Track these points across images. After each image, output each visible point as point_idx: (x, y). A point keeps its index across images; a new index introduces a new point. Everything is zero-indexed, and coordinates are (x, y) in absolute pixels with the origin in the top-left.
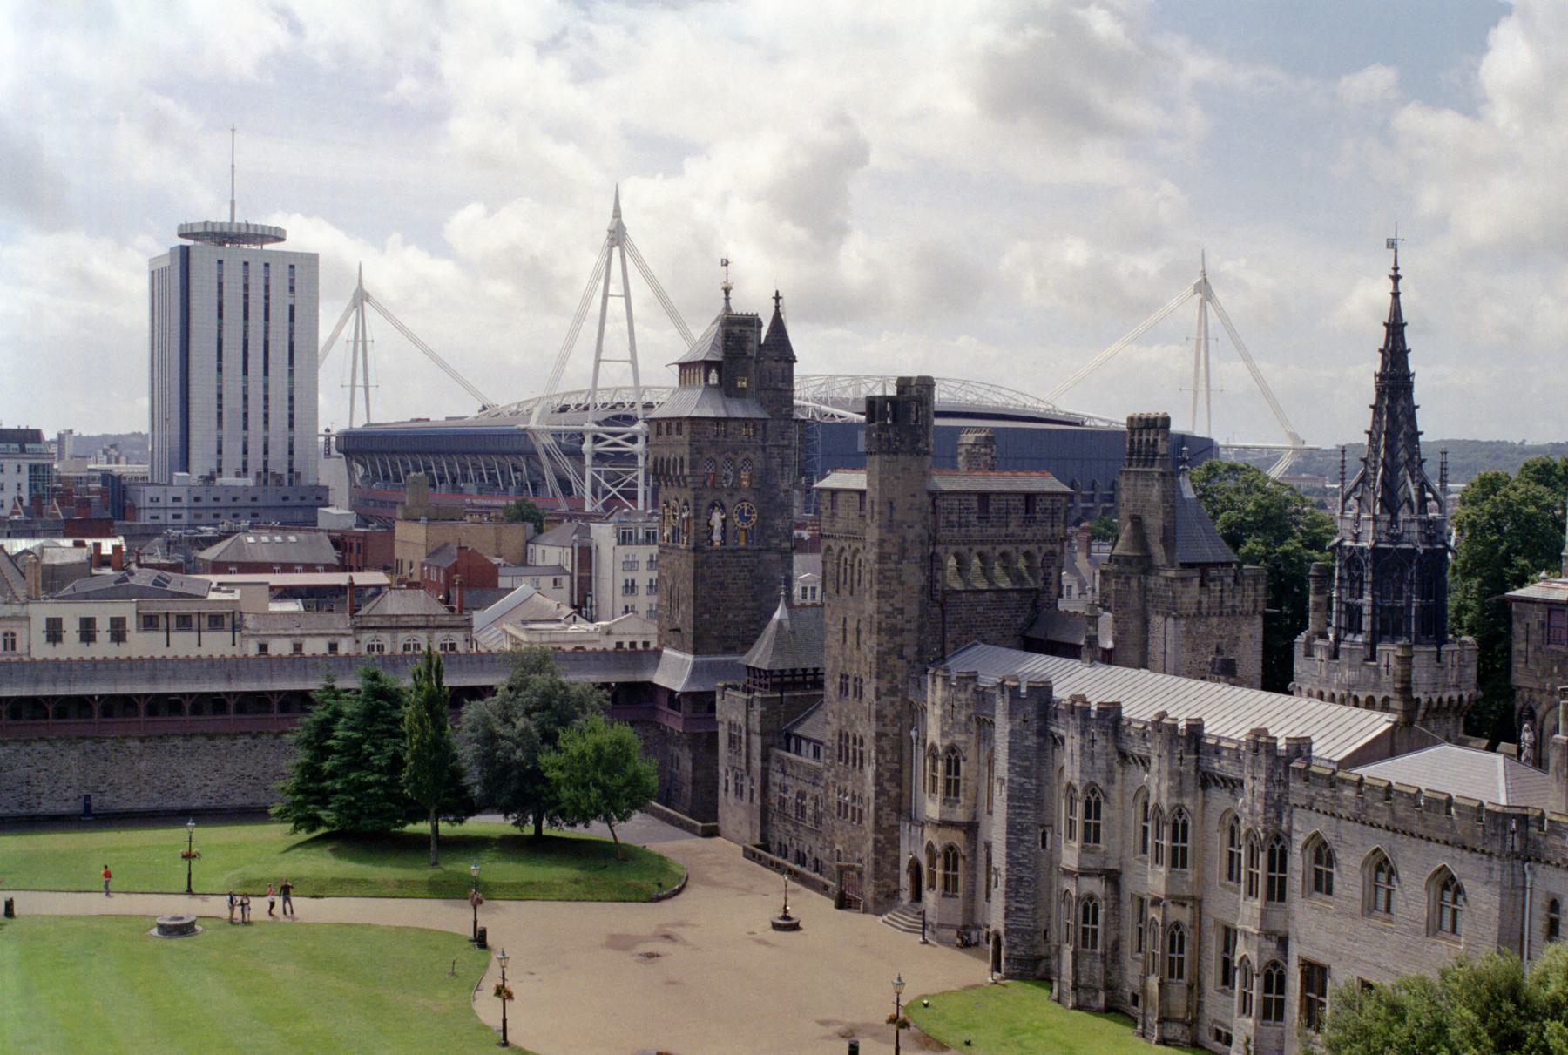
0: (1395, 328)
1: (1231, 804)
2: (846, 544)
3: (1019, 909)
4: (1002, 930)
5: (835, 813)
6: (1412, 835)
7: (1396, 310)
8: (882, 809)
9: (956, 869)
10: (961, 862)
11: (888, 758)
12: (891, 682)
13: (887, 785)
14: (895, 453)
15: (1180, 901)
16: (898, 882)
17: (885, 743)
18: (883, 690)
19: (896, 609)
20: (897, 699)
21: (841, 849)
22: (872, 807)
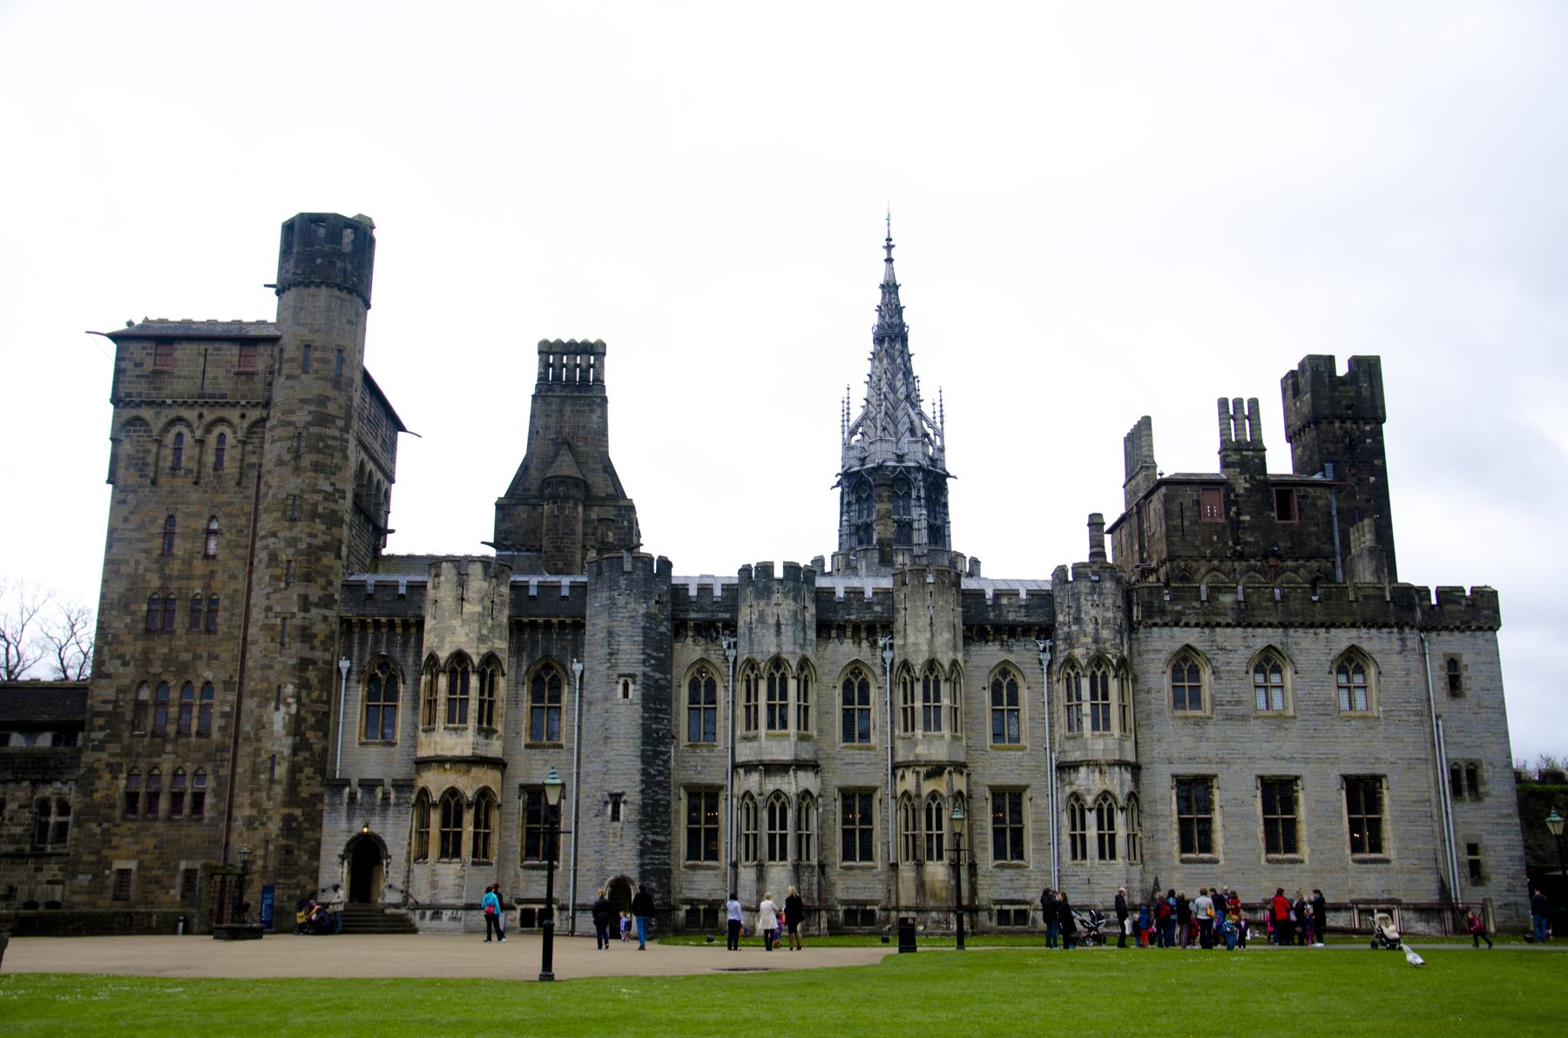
0: (890, 288)
1: (1003, 656)
2: (190, 415)
3: (654, 842)
4: (633, 873)
5: (118, 813)
6: (1312, 626)
7: (891, 273)
8: (302, 771)
9: (487, 826)
10: (495, 816)
11: (315, 695)
12: (324, 588)
13: (310, 735)
14: (350, 292)
15: (960, 767)
16: (316, 880)
17: (312, 675)
18: (314, 598)
19: (338, 490)
20: (330, 613)
21: (132, 865)
22: (281, 771)
